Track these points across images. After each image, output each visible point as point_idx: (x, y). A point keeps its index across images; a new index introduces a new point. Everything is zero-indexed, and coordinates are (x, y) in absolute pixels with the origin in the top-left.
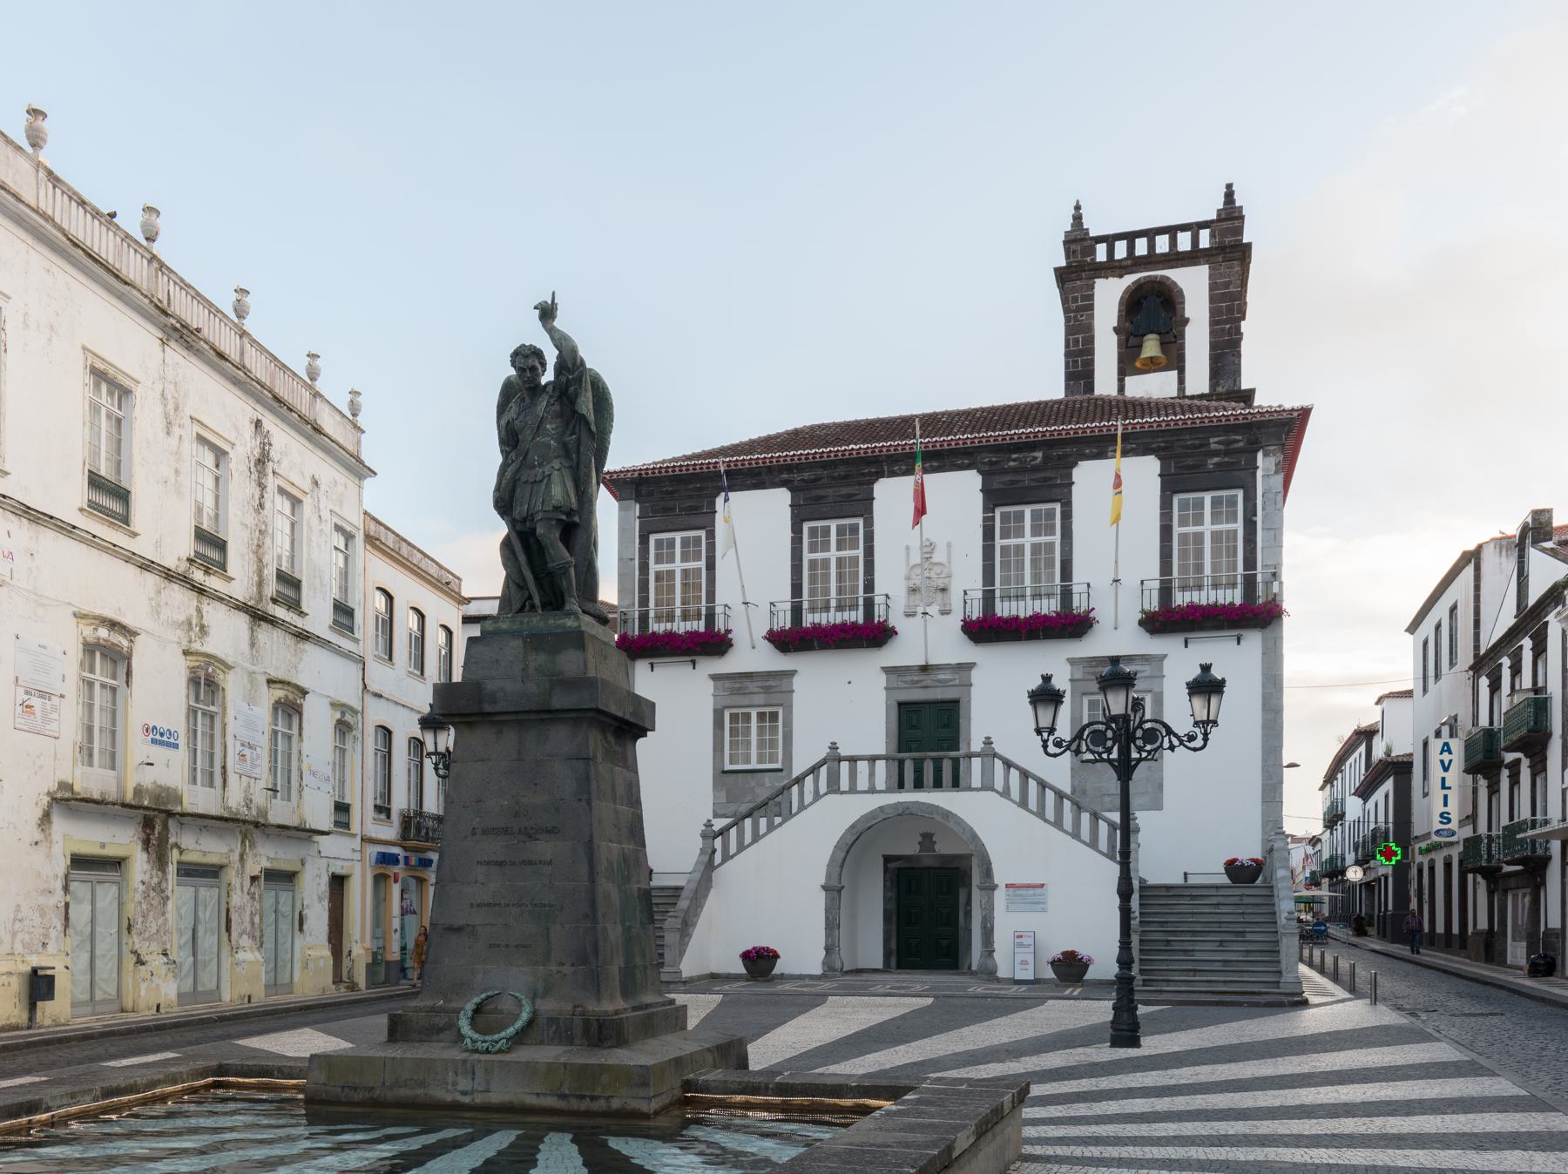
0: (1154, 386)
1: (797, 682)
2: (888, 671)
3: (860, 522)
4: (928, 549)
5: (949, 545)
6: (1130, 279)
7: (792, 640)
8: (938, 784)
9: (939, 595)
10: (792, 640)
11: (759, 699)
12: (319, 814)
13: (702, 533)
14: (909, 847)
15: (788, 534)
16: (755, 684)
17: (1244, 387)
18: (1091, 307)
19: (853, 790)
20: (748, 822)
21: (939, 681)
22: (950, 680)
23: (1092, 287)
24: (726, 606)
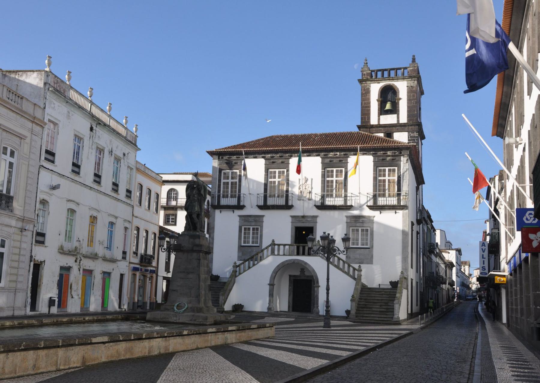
0: (389, 119)
1: (265, 219)
2: (292, 217)
3: (285, 170)
5: (312, 179)
8: (304, 254)
11: (253, 224)
12: (119, 256)
16: (252, 219)
19: (278, 255)
20: (247, 263)
21: (308, 221)
22: (310, 221)
24: (244, 194)
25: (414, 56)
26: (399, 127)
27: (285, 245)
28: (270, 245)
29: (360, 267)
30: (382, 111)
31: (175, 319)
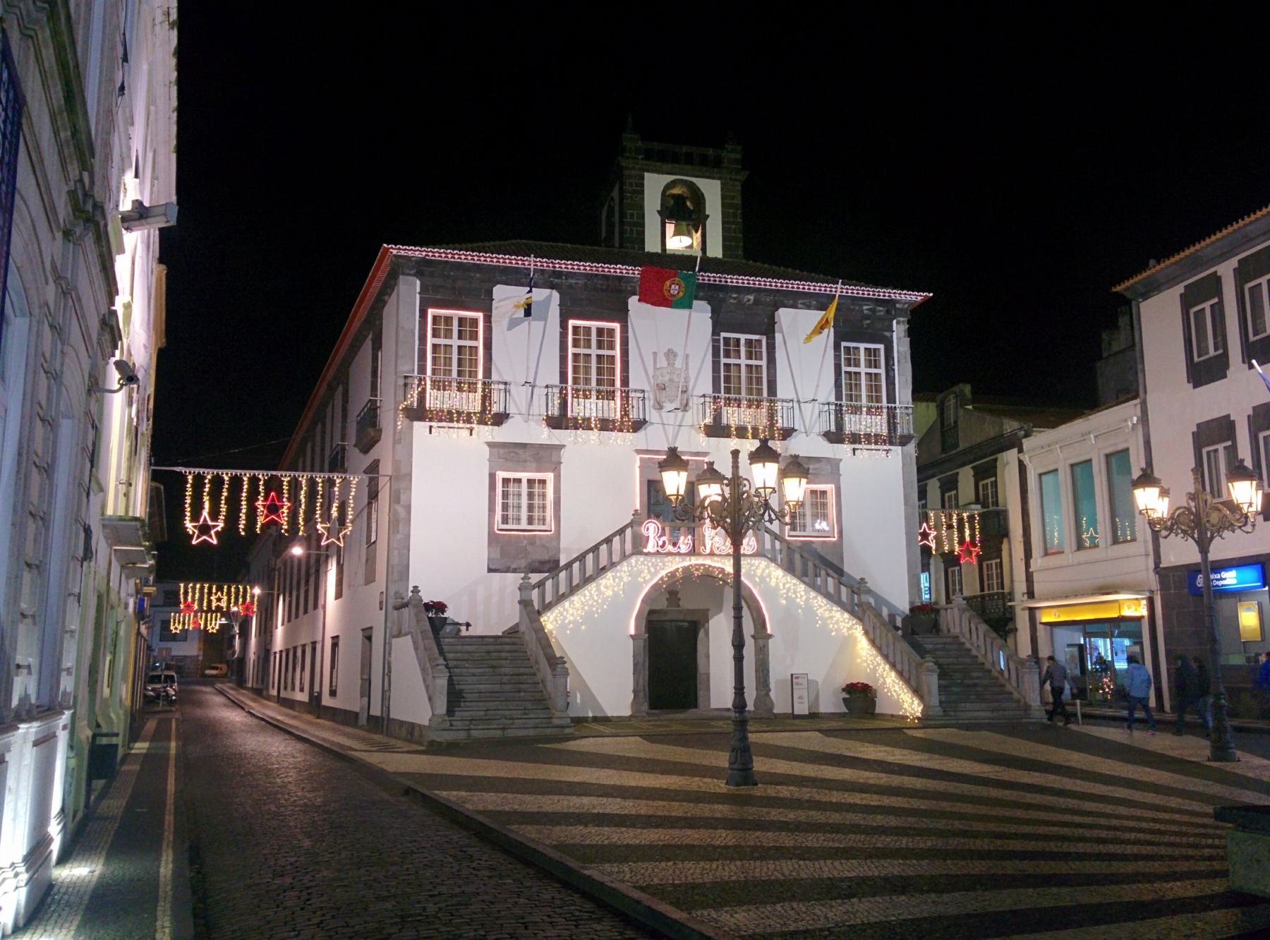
13: (480, 316)
15: (558, 329)
18: (642, 192)
28: (631, 525)
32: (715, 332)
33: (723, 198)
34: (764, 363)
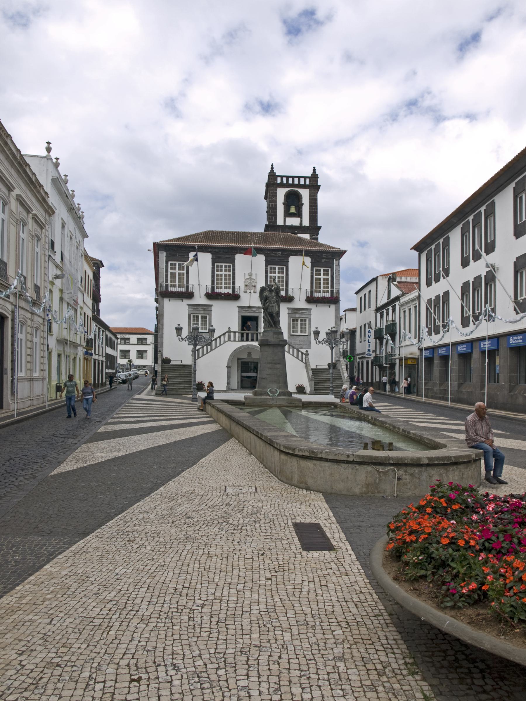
1: (213, 308)
2: (239, 307)
4: (250, 275)
6: (287, 189)
7: (212, 296)
9: (253, 288)
10: (212, 296)
11: (202, 312)
14: (244, 356)
15: (211, 266)
17: (319, 225)
18: (276, 196)
19: (235, 341)
23: (277, 190)
25: (314, 168)
26: (301, 229)
27: (235, 332)
29: (307, 351)
30: (287, 214)
31: (273, 402)
32: (267, 265)
33: (310, 196)
34: (284, 275)
